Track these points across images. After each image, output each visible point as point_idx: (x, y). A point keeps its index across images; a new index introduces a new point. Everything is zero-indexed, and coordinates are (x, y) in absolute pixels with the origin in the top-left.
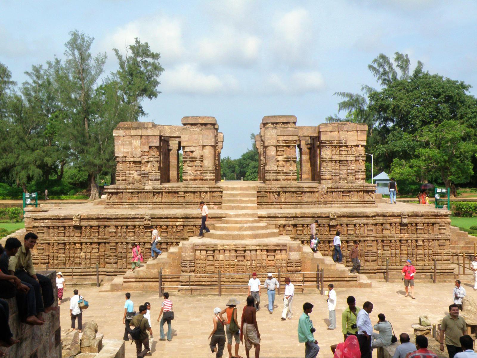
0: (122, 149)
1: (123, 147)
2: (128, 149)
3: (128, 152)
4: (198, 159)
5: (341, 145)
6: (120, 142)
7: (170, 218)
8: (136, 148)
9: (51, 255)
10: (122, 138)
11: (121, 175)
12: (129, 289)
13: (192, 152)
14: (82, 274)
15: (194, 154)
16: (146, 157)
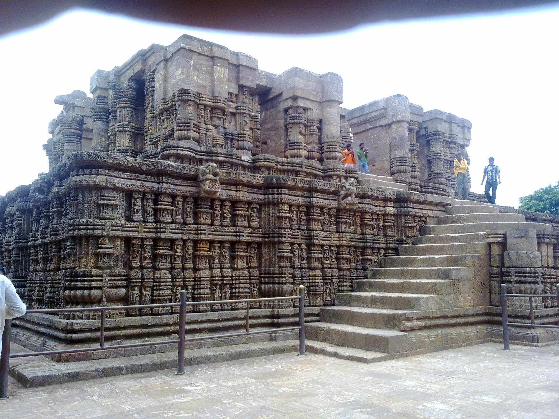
0: (195, 78)
1: (196, 73)
2: (204, 80)
3: (204, 87)
4: (316, 124)
5: (453, 140)
6: (192, 62)
7: (377, 198)
8: (220, 81)
9: (136, 274)
10: (195, 57)
11: (192, 126)
12: (419, 347)
13: (305, 109)
14: (221, 325)
15: (309, 114)
16: (233, 105)
